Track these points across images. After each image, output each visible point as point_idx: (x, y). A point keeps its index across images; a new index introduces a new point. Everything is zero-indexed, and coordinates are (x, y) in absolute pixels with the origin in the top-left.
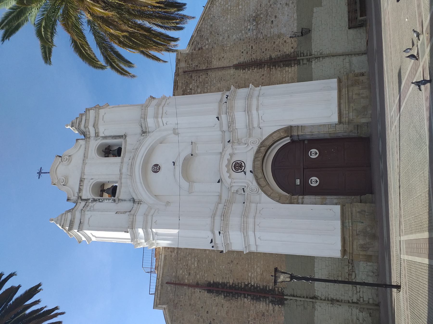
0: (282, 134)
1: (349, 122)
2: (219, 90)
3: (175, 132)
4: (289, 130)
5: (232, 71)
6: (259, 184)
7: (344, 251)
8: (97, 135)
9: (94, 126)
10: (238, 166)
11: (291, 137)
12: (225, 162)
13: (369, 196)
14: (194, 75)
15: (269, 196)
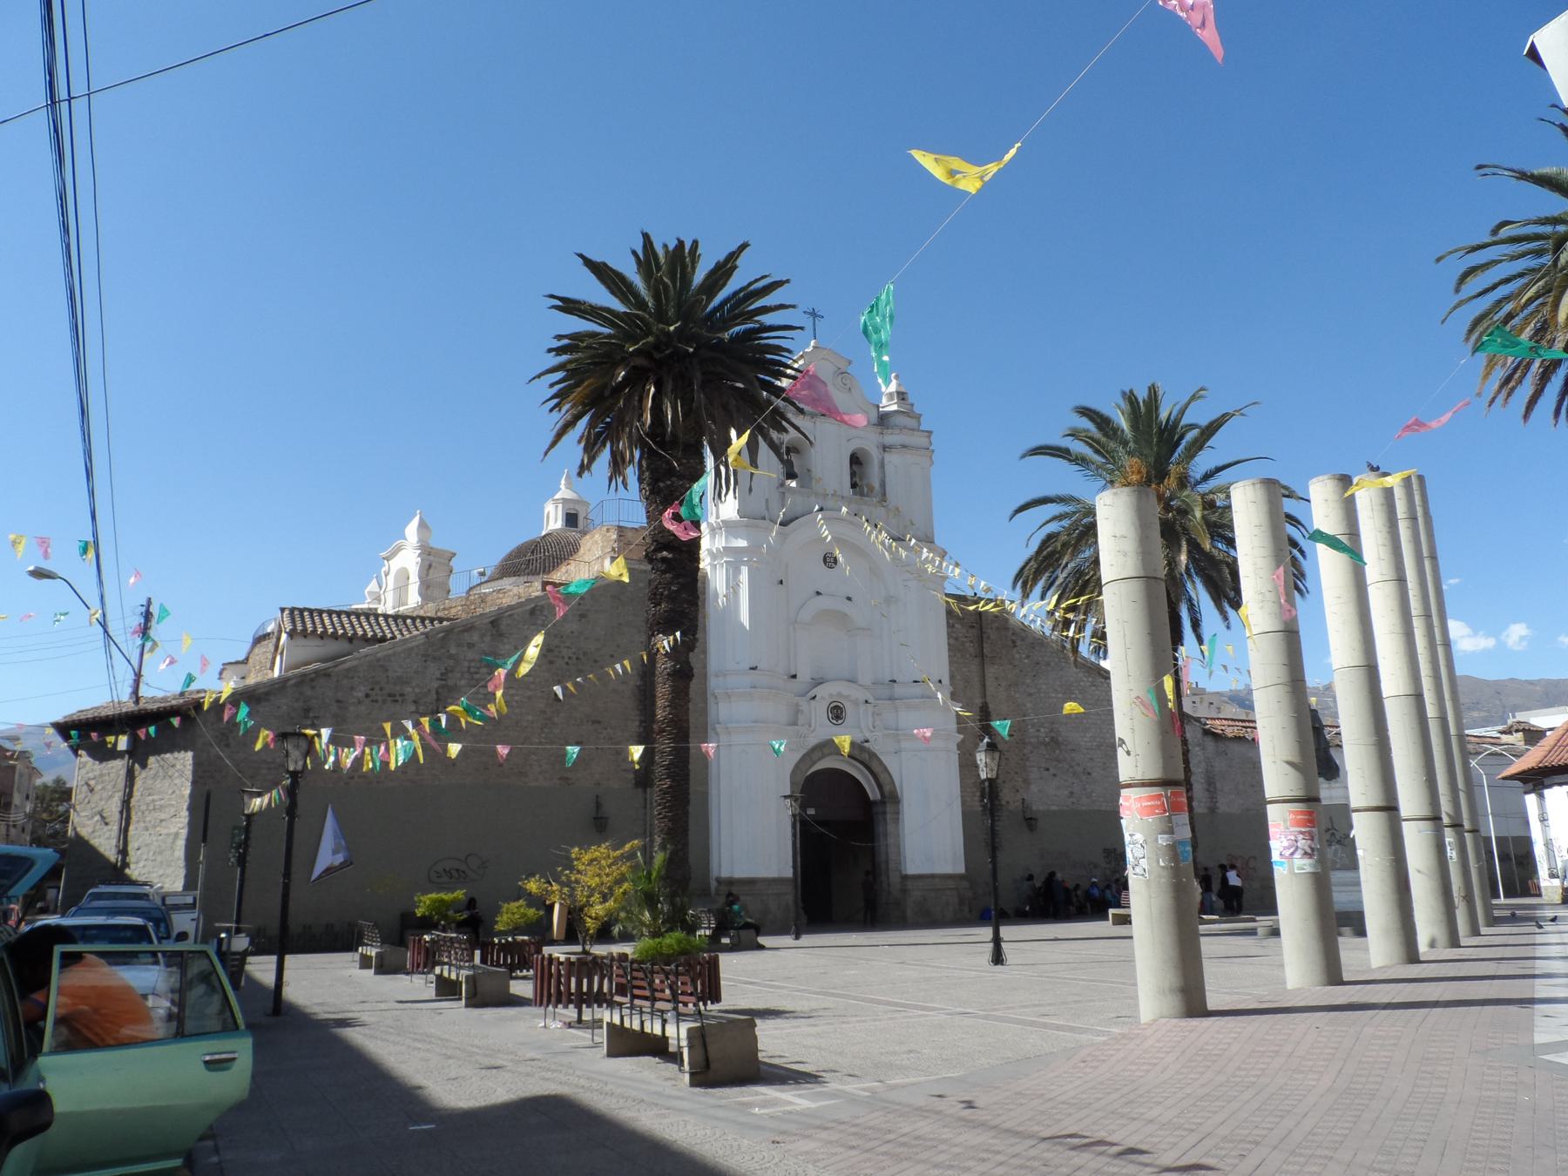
0: (887, 788)
1: (904, 891)
2: (952, 677)
3: (889, 600)
4: (891, 798)
5: (978, 701)
6: (814, 749)
7: (731, 882)
8: (885, 448)
9: (904, 446)
10: (837, 713)
11: (883, 802)
12: (845, 693)
13: (804, 919)
14: (975, 632)
15: (797, 766)
